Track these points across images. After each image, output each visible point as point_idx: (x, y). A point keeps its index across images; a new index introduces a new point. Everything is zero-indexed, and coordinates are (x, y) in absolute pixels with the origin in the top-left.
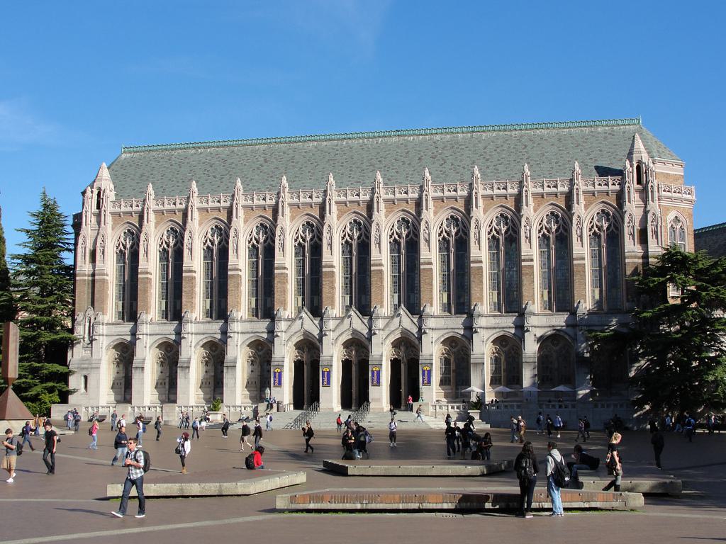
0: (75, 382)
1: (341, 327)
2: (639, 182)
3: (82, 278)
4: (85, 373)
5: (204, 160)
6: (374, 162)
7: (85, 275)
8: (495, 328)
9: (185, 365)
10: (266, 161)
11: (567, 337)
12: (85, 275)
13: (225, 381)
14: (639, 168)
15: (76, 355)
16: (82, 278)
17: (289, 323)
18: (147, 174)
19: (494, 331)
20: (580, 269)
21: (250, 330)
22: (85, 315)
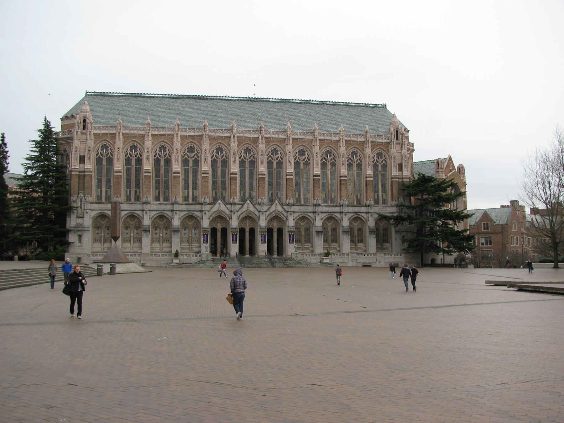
0: (72, 238)
1: (242, 209)
2: (397, 139)
3: (75, 173)
4: (80, 233)
5: (143, 105)
6: (249, 115)
7: (76, 171)
8: (326, 212)
9: (147, 229)
10: (184, 109)
11: (363, 218)
12: (76, 171)
13: (173, 239)
14: (397, 131)
15: (72, 221)
16: (75, 173)
17: (211, 206)
18: (108, 110)
19: (326, 214)
20: (370, 183)
21: (186, 210)
22: (78, 197)
